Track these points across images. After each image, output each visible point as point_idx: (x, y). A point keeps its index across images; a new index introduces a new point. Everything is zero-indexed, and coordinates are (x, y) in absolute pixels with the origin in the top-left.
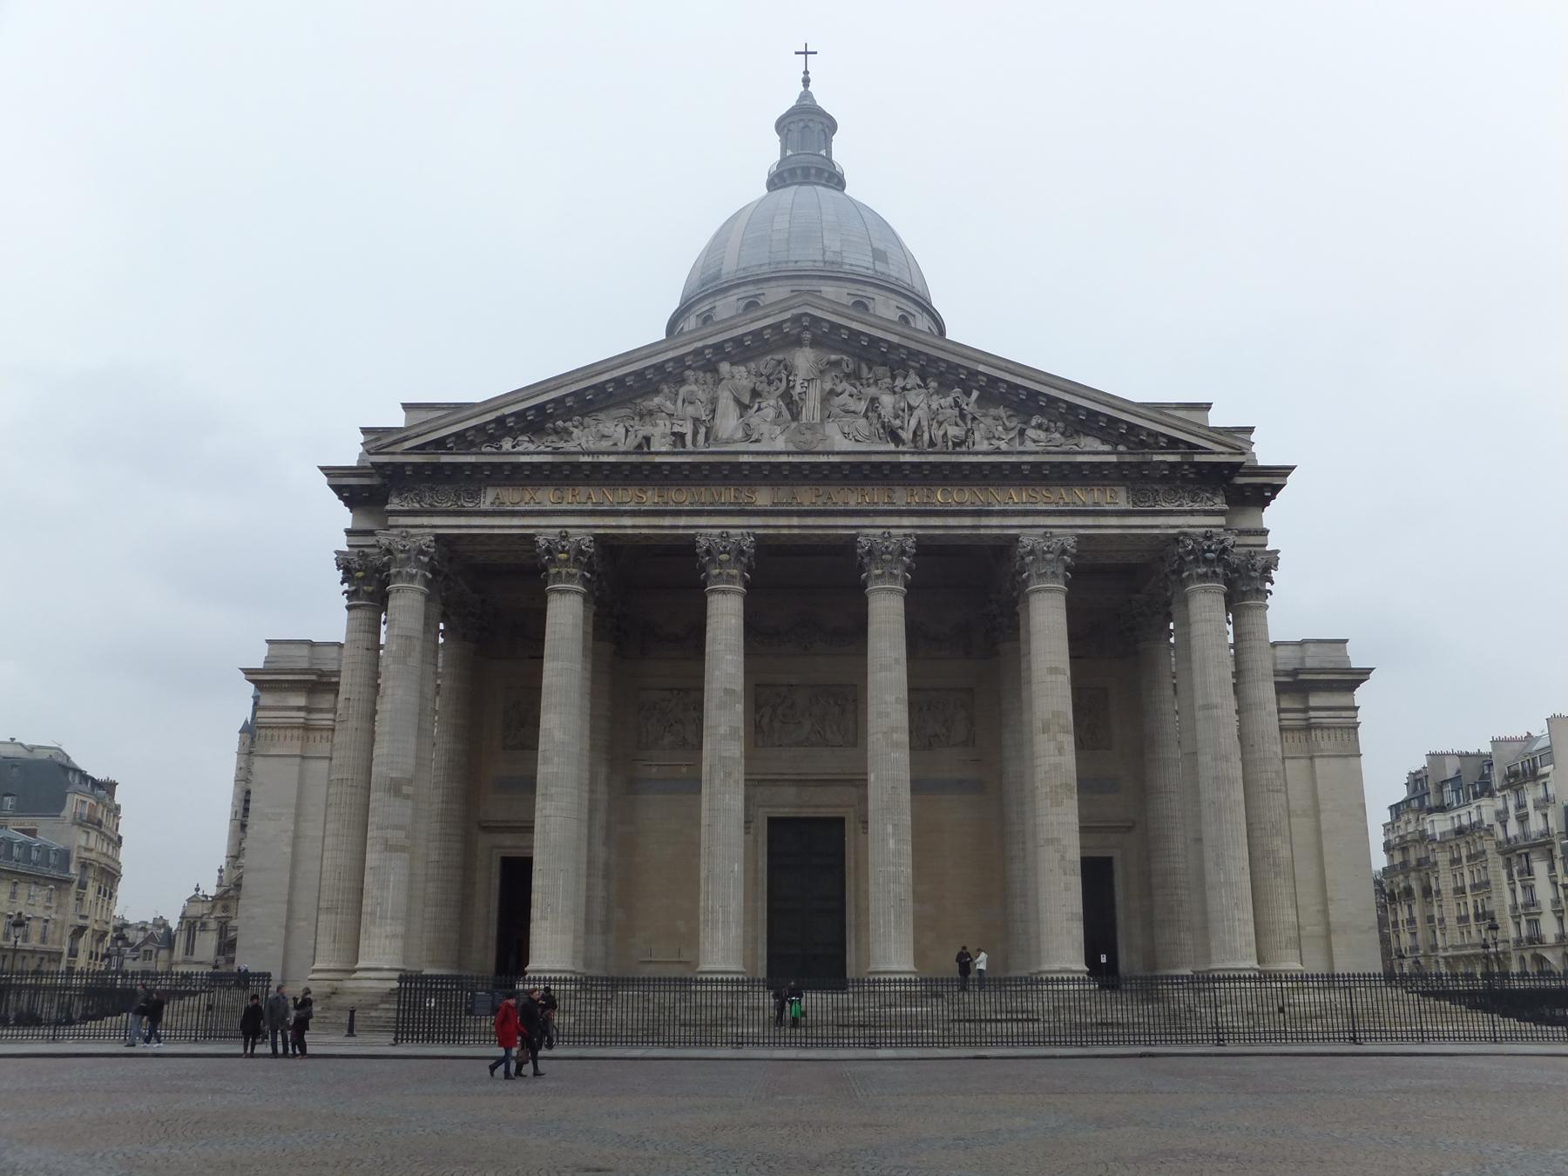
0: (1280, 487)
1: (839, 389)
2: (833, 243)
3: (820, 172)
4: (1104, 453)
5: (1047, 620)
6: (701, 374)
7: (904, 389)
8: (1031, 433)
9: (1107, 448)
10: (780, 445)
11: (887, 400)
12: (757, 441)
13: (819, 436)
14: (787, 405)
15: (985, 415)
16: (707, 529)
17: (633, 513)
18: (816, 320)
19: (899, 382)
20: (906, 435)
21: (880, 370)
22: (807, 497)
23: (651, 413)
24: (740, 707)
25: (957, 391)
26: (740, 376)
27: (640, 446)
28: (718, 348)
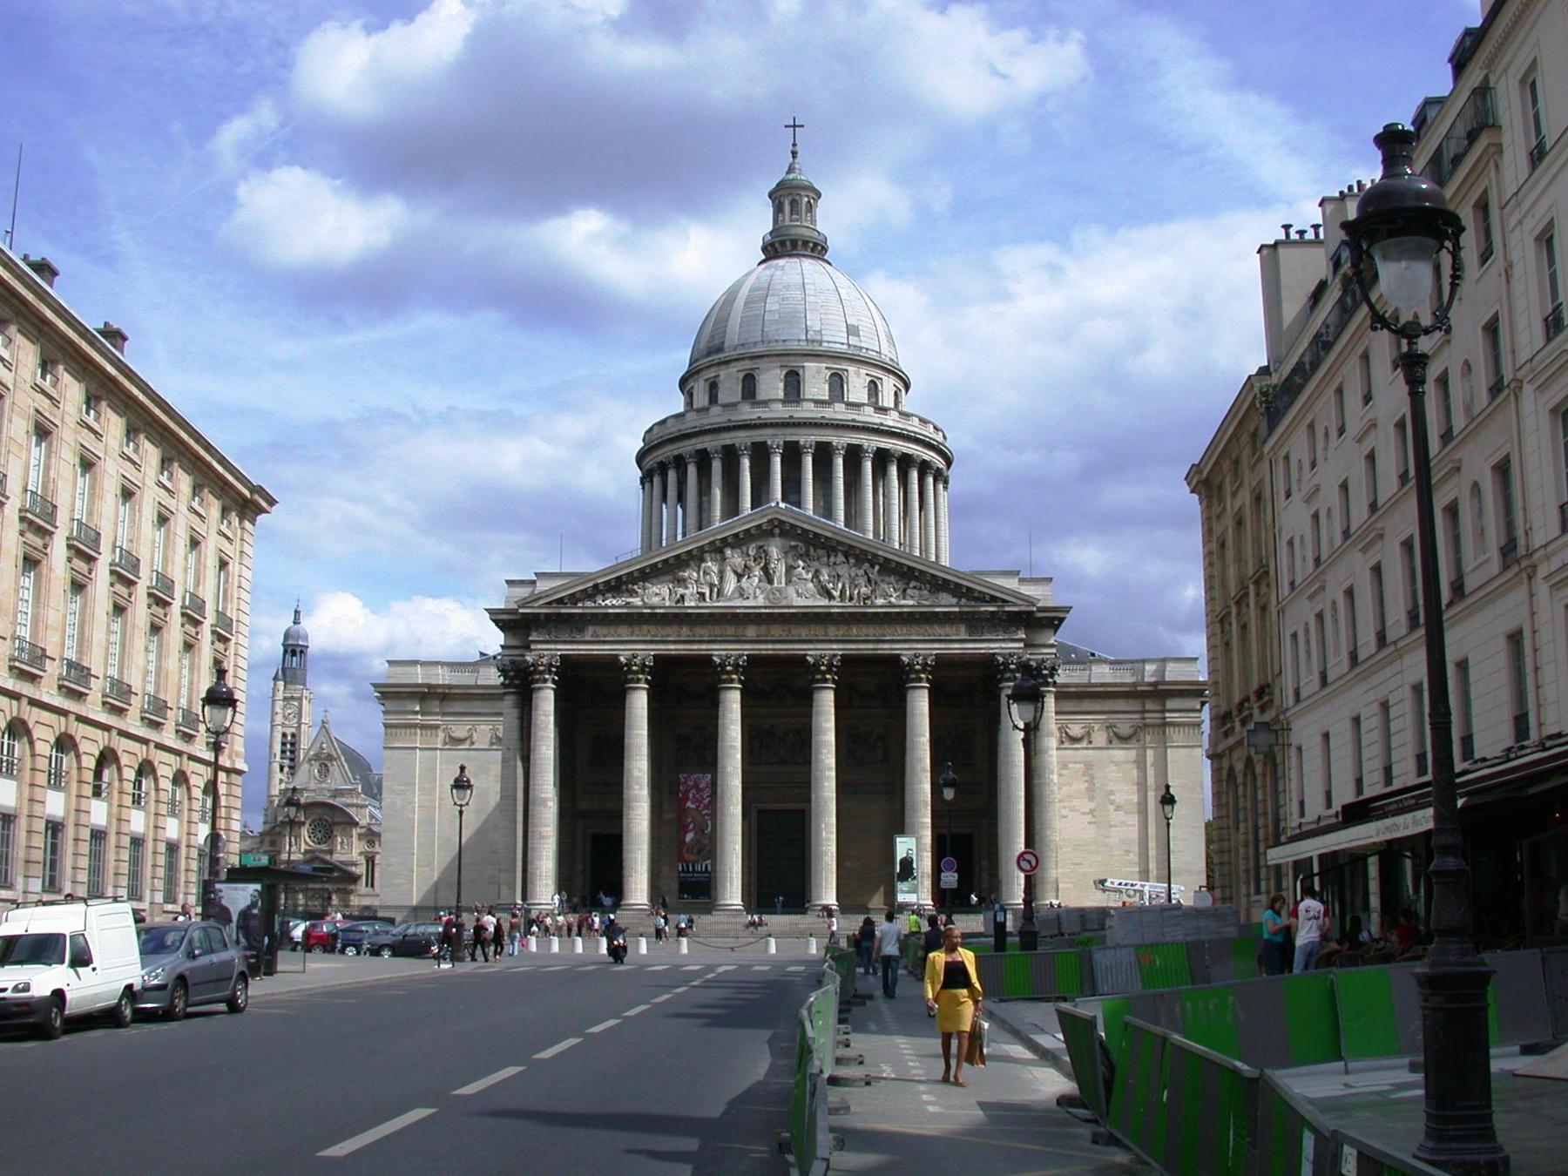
0: (1062, 620)
2: (814, 322)
3: (805, 243)
5: (920, 704)
9: (954, 601)
10: (761, 601)
16: (718, 651)
17: (675, 642)
18: (782, 522)
19: (832, 559)
20: (836, 594)
21: (821, 552)
22: (777, 631)
23: (684, 580)
24: (739, 756)
26: (735, 558)
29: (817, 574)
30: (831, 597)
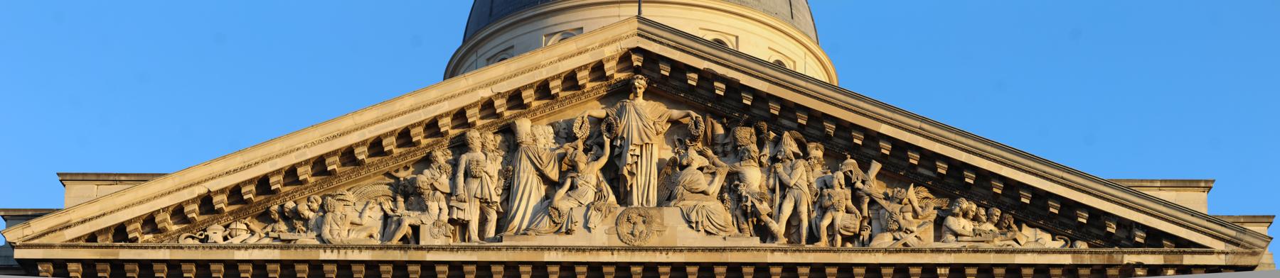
1: (685, 162)
4: (1054, 252)
6: (491, 136)
7: (774, 159)
8: (952, 222)
9: (1059, 244)
11: (754, 177)
12: (568, 232)
13: (655, 226)
14: (610, 182)
15: (887, 197)
18: (652, 60)
19: (767, 151)
20: (779, 227)
25: (851, 163)
27: (404, 239)
28: (515, 99)
29: (734, 179)
30: (764, 233)
